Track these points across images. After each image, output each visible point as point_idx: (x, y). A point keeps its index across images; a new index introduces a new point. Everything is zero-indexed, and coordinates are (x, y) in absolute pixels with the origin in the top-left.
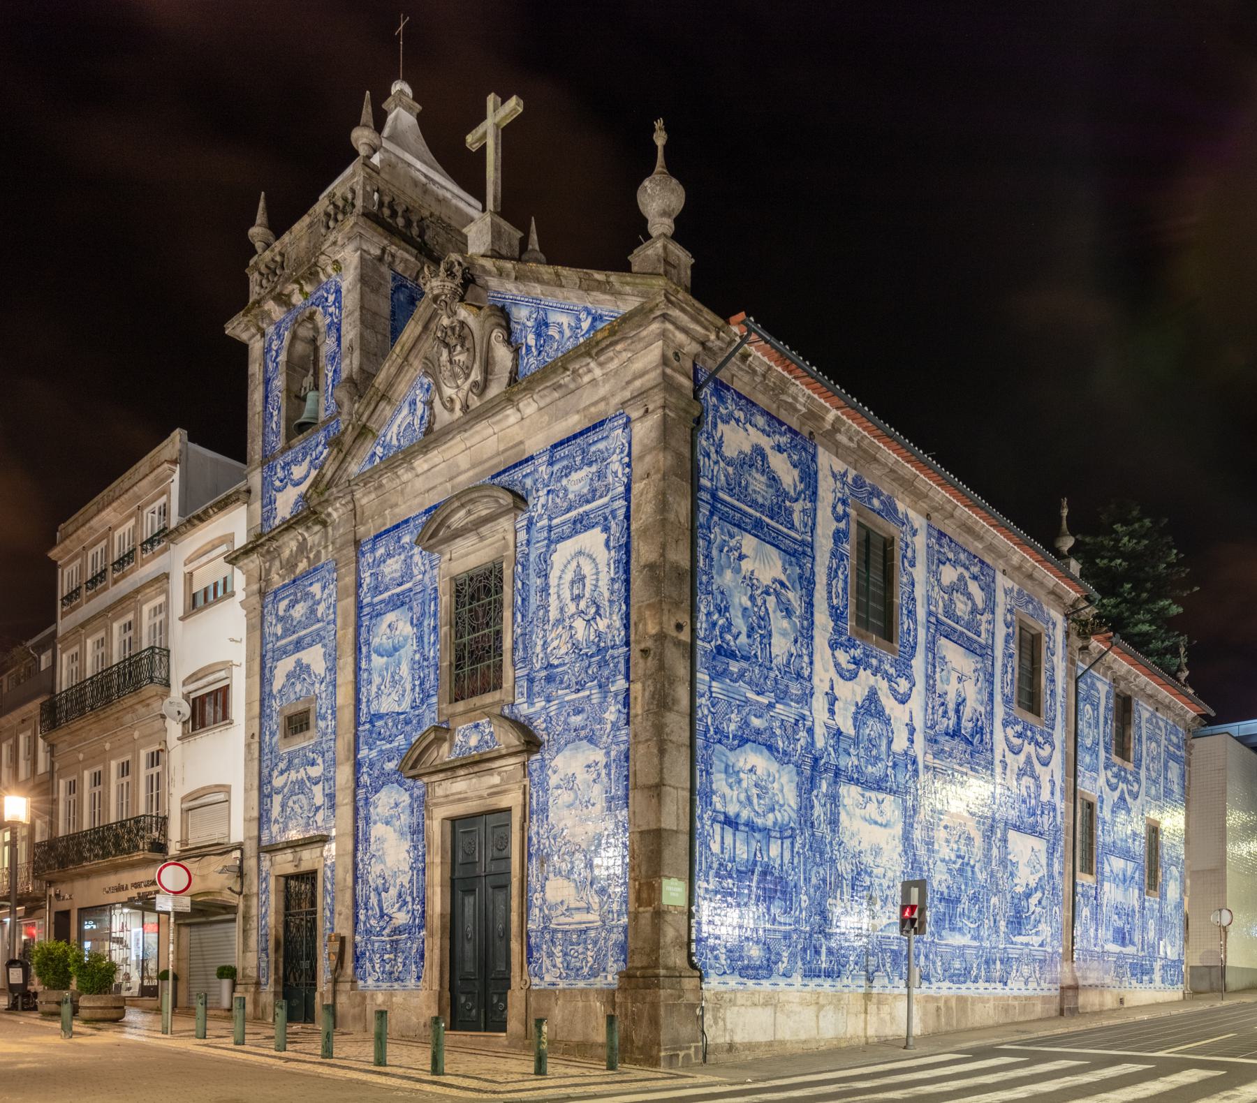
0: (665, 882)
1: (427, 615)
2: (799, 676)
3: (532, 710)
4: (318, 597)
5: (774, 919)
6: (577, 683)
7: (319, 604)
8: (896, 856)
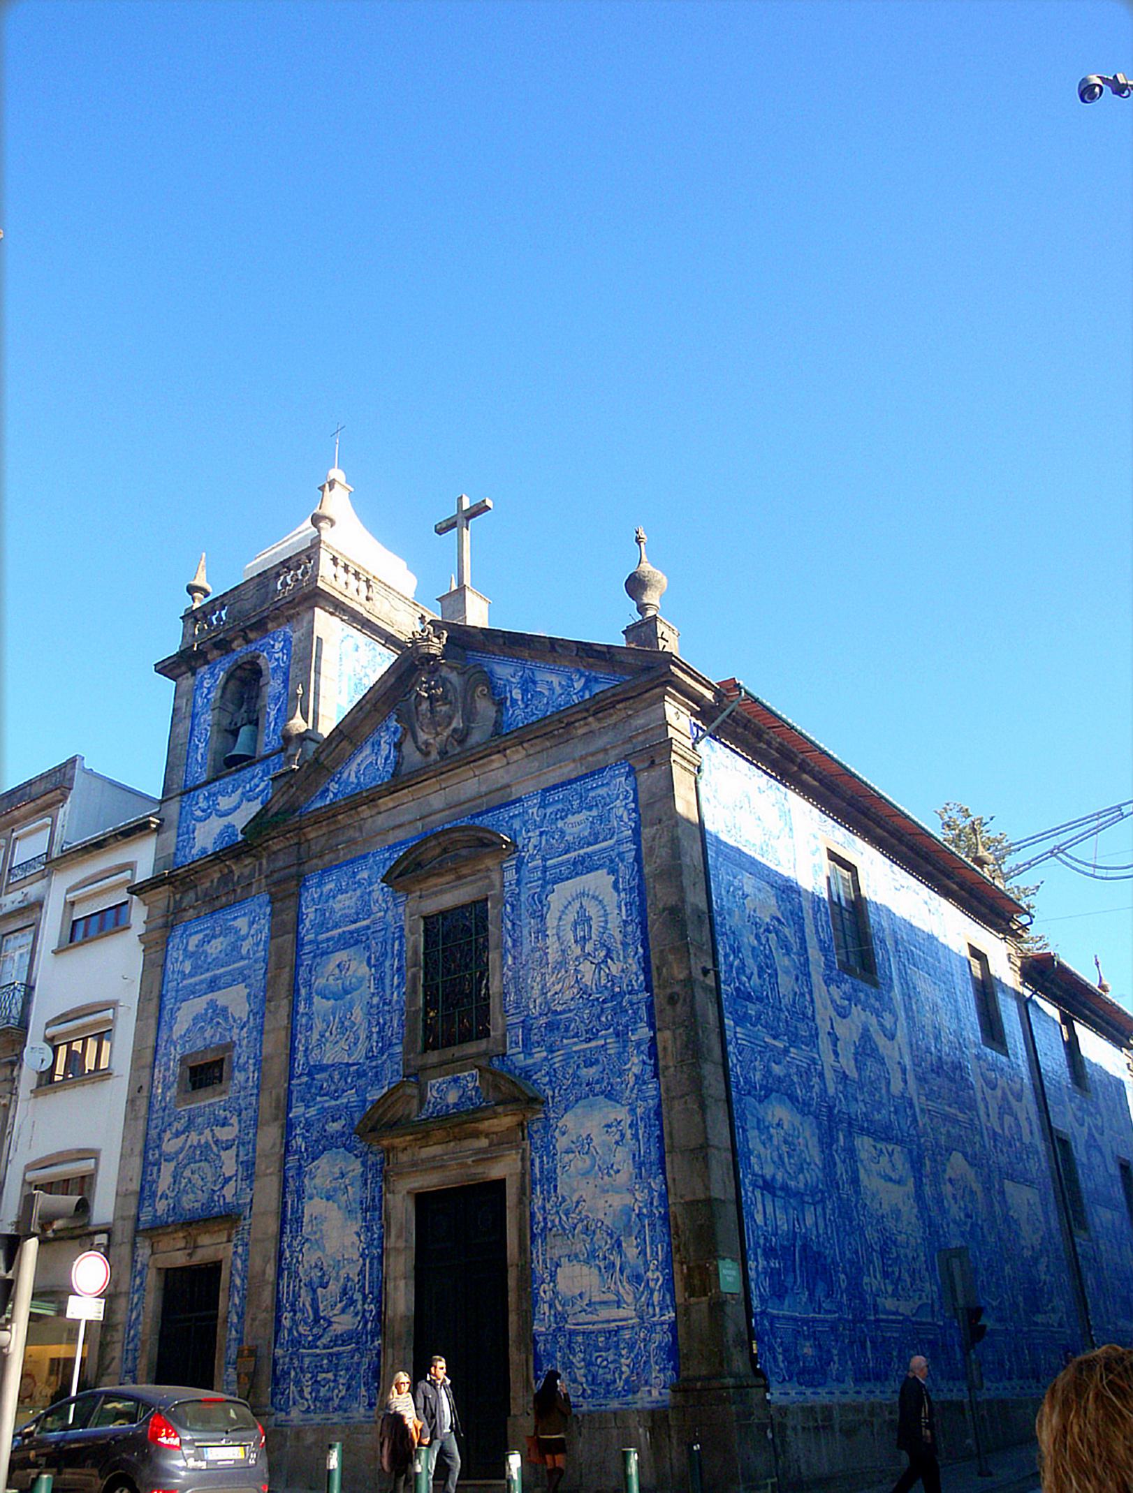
0: (721, 1263)
1: (390, 955)
2: (804, 1015)
3: (530, 1061)
4: (242, 933)
5: (820, 1306)
8: (914, 1220)
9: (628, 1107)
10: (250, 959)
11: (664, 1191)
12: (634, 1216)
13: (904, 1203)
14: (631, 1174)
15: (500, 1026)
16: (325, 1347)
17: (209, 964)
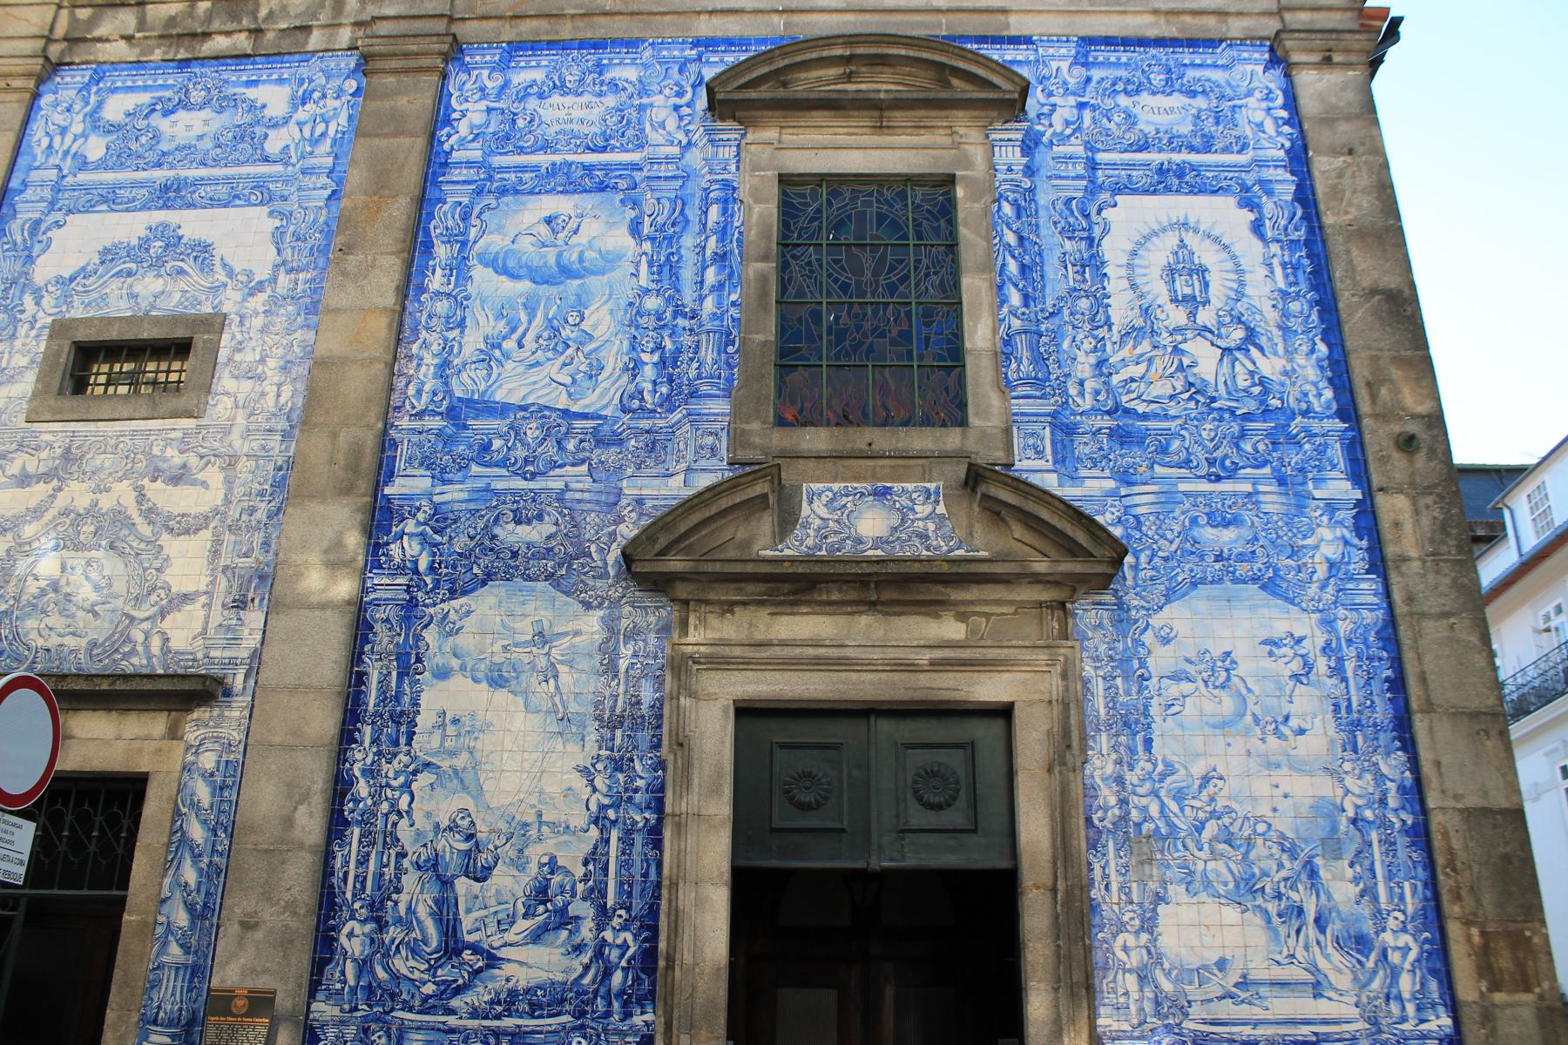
6: (1211, 462)
7: (275, 126)
9: (1318, 615)
10: (286, 164)
11: (1408, 783)
12: (1343, 824)
14: (1332, 741)
15: (995, 411)
16: (474, 1014)
17: (164, 154)
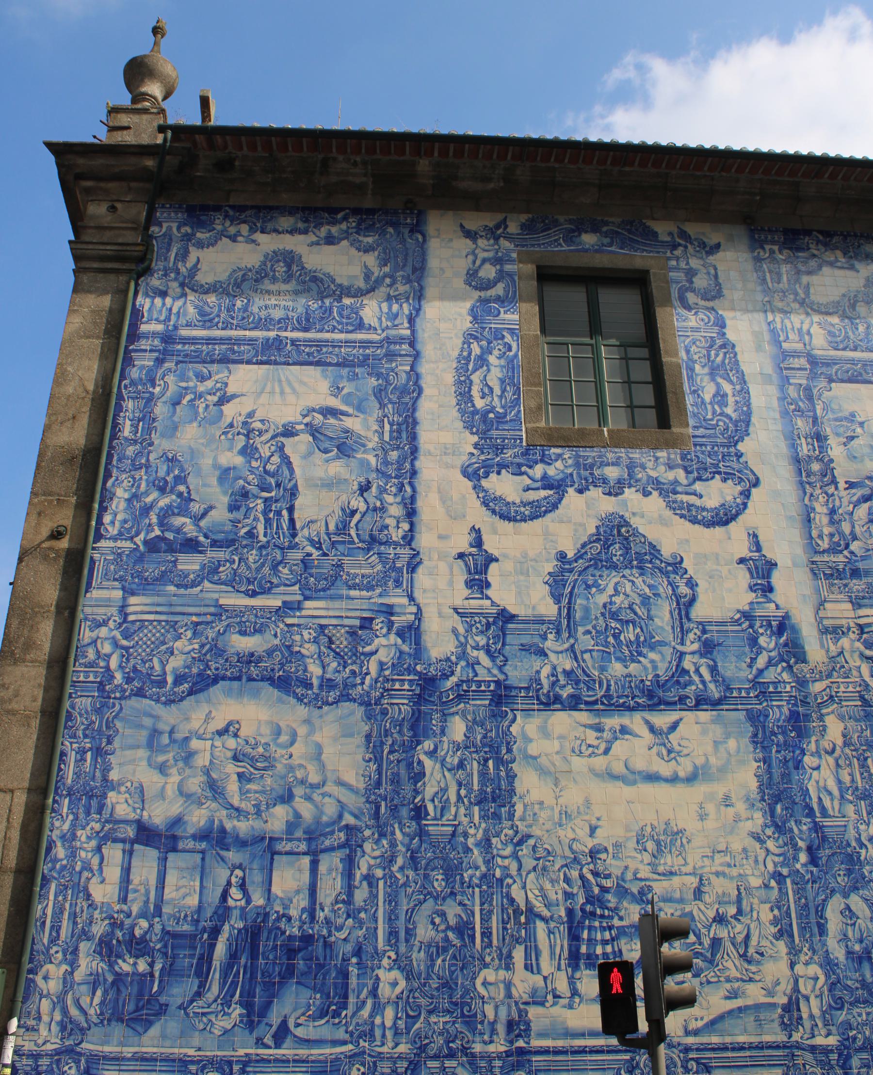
13: (703, 817)
